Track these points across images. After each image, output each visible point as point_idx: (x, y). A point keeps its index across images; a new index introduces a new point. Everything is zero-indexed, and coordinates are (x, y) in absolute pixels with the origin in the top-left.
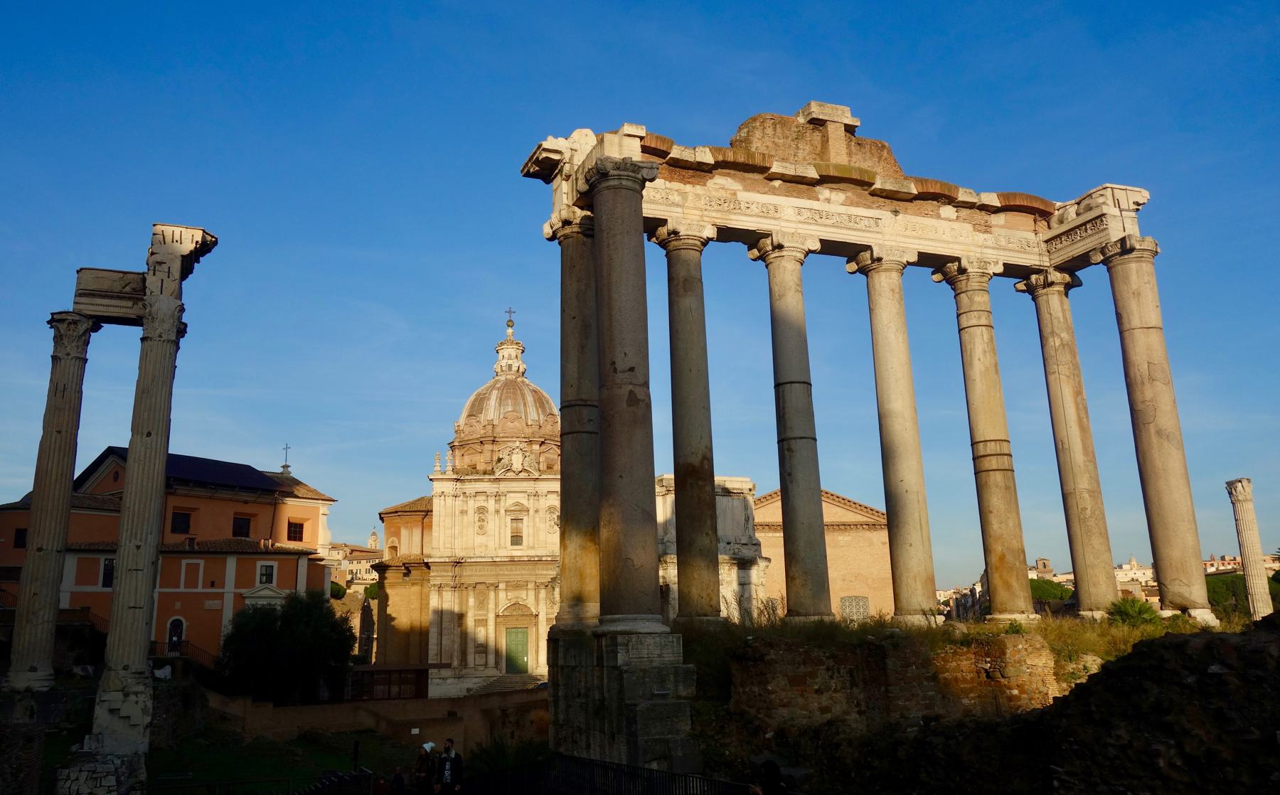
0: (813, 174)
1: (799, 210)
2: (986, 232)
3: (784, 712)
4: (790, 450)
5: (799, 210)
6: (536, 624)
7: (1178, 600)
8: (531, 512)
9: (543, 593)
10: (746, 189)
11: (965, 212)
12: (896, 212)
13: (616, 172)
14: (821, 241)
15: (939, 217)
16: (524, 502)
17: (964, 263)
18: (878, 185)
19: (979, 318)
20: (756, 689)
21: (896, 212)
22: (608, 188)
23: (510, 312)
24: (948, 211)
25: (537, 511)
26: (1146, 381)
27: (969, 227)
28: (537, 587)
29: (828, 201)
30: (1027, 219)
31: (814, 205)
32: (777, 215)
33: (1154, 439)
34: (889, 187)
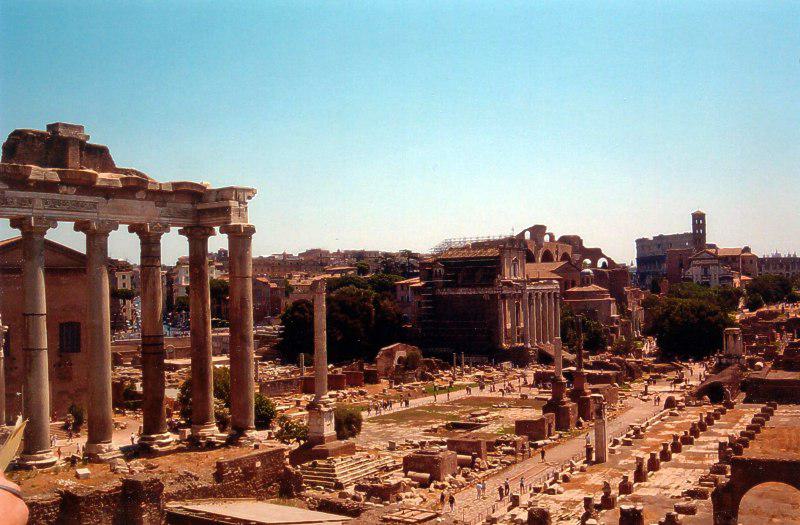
0: (56, 178)
1: (45, 201)
2: (162, 206)
5: (45, 201)
10: (11, 188)
12: (107, 198)
15: (134, 198)
18: (98, 184)
21: (107, 198)
24: (140, 194)
27: (152, 203)
31: (56, 196)
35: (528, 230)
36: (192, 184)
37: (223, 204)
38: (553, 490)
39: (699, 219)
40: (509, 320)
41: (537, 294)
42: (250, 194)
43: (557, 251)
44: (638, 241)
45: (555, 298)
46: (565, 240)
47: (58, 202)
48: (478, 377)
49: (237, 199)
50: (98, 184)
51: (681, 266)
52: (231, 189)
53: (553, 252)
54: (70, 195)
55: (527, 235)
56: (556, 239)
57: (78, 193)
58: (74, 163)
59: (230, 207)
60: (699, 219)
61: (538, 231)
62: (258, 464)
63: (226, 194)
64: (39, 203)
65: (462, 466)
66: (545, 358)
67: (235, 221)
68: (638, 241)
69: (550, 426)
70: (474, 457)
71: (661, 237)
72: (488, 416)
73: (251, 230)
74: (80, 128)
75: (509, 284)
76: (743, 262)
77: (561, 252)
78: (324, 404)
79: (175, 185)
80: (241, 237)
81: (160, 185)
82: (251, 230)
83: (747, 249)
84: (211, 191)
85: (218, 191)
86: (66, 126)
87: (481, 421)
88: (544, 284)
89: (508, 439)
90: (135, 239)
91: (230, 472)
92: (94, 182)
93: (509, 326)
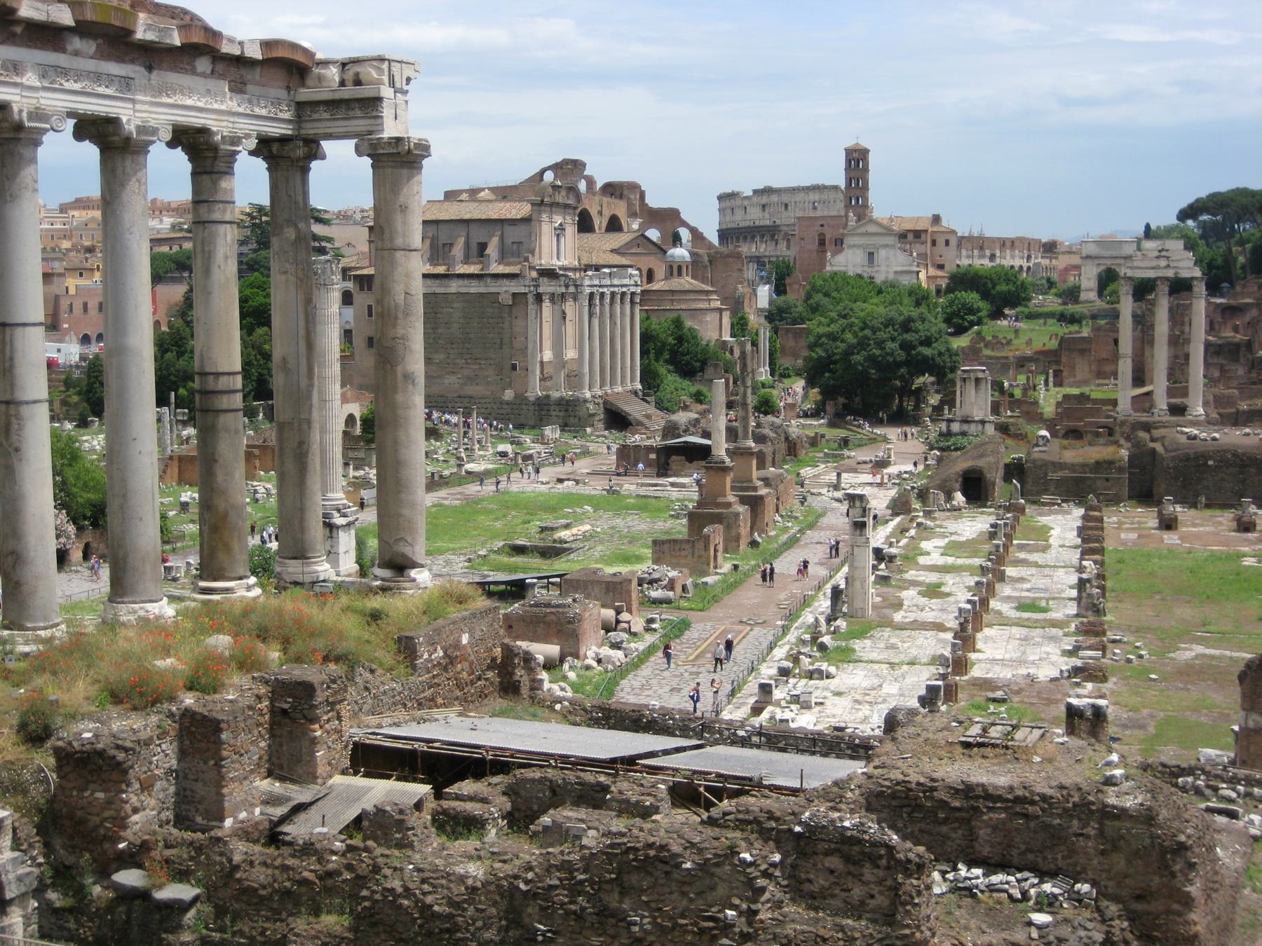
0: (64, 16)
3: (135, 818)
4: (18, 417)
7: (400, 561)
11: (220, 67)
12: (150, 69)
14: (71, 114)
15: (194, 72)
18: (141, 34)
19: (224, 211)
20: (100, 795)
21: (150, 69)
24: (203, 64)
26: (400, 315)
29: (76, 53)
30: (279, 75)
33: (400, 385)
34: (150, 36)
35: (549, 168)
36: (295, 47)
37: (364, 92)
38: (820, 672)
39: (857, 160)
40: (547, 343)
41: (602, 294)
42: (408, 72)
43: (600, 213)
44: (721, 198)
45: (632, 302)
46: (613, 189)
48: (504, 454)
49: (392, 83)
50: (139, 35)
51: (822, 242)
52: (382, 59)
53: (593, 212)
55: (549, 176)
56: (599, 185)
57: (101, 55)
60: (857, 160)
61: (570, 168)
62: (465, 639)
65: (608, 628)
66: (617, 420)
67: (390, 129)
68: (721, 198)
69: (716, 551)
70: (618, 611)
71: (768, 191)
72: (574, 531)
73: (424, 149)
75: (549, 274)
76: (934, 243)
77: (607, 214)
78: (339, 511)
79: (267, 45)
80: (396, 161)
81: (241, 43)
82: (424, 149)
83: (936, 219)
84: (325, 63)
85: (344, 65)
87: (562, 541)
89: (656, 575)
90: (179, 162)
91: (426, 656)
92: (130, 32)
93: (548, 355)
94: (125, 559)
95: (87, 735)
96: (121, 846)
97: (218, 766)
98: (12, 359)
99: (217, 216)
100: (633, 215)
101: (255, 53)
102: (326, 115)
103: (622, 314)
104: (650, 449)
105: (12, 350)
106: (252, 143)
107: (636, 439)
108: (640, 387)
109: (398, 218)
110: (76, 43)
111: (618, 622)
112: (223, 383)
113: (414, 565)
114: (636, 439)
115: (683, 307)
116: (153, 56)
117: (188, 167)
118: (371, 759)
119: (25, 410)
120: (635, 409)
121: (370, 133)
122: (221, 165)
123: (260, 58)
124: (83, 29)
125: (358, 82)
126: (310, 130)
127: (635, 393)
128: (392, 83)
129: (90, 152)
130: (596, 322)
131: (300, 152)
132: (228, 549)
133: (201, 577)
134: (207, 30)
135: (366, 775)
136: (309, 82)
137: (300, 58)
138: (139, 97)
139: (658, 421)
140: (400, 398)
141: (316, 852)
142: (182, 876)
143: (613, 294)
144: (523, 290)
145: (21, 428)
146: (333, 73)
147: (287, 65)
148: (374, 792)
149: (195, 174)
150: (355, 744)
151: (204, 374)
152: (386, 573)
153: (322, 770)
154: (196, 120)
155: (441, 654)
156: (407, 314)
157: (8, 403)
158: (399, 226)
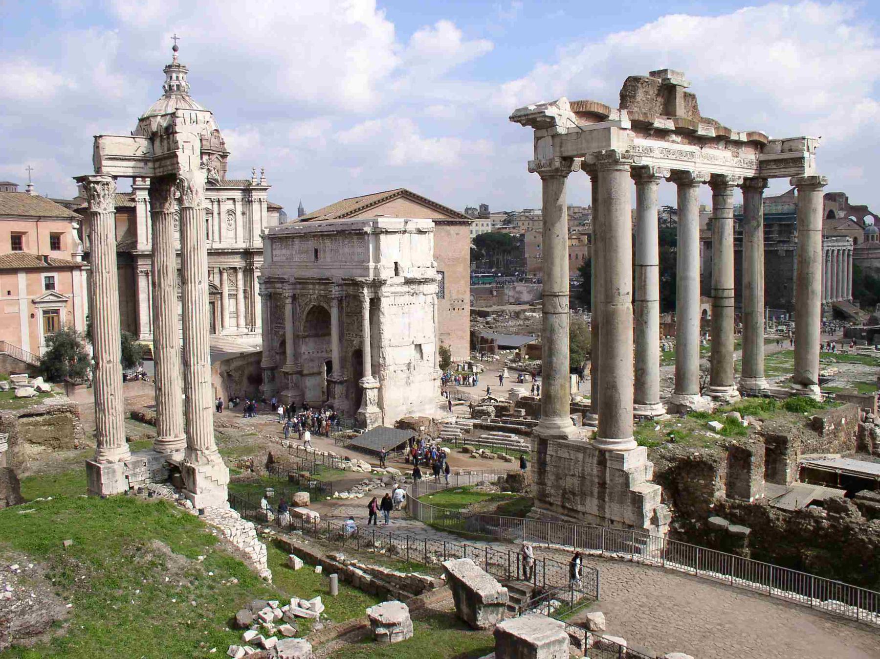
0: (670, 125)
4: (647, 307)
6: (221, 300)
8: (216, 215)
9: (225, 276)
13: (623, 160)
16: (210, 207)
17: (728, 179)
18: (701, 132)
20: (702, 482)
22: (617, 170)
23: (175, 38)
24: (721, 146)
25: (219, 214)
28: (221, 273)
29: (673, 142)
32: (651, 155)
36: (760, 134)
45: (848, 255)
47: (668, 151)
54: (677, 144)
58: (681, 109)
59: (803, 158)
63: (794, 145)
64: (657, 153)
67: (808, 172)
74: (682, 74)
79: (749, 135)
84: (774, 142)
85: (783, 142)
86: (673, 72)
88: (836, 240)
94: (684, 375)
95: (697, 454)
96: (712, 506)
97: (749, 472)
98: (645, 281)
99: (725, 215)
100: (841, 209)
101: (744, 138)
102: (774, 166)
103: (843, 260)
104: (862, 330)
105: (645, 278)
106: (741, 182)
107: (849, 325)
108: (851, 298)
109: (812, 216)
110: (674, 137)
111: (866, 418)
112: (726, 294)
113: (813, 383)
114: (849, 325)
115: (874, 256)
116: (702, 141)
117: (712, 193)
118: (811, 475)
119: (650, 304)
120: (851, 310)
121: (798, 174)
122: (728, 192)
123: (746, 140)
124: (679, 131)
125: (791, 150)
126: (765, 173)
127: (849, 301)
128: (808, 150)
129: (673, 187)
130: (829, 264)
131: (761, 184)
132: (726, 372)
133: (711, 385)
134: (726, 129)
135: (809, 483)
136: (765, 150)
137: (762, 139)
138: (698, 160)
139: (863, 317)
140: (809, 302)
141: (813, 517)
142: (741, 522)
143: (839, 250)
144: (791, 249)
145: (648, 312)
146: (779, 147)
147: (758, 144)
148: (815, 492)
149: (714, 196)
150: (803, 468)
151: (716, 290)
152: (798, 387)
153: (788, 479)
154: (718, 171)
155: (833, 427)
156: (815, 261)
157: (642, 301)
158: (812, 219)
